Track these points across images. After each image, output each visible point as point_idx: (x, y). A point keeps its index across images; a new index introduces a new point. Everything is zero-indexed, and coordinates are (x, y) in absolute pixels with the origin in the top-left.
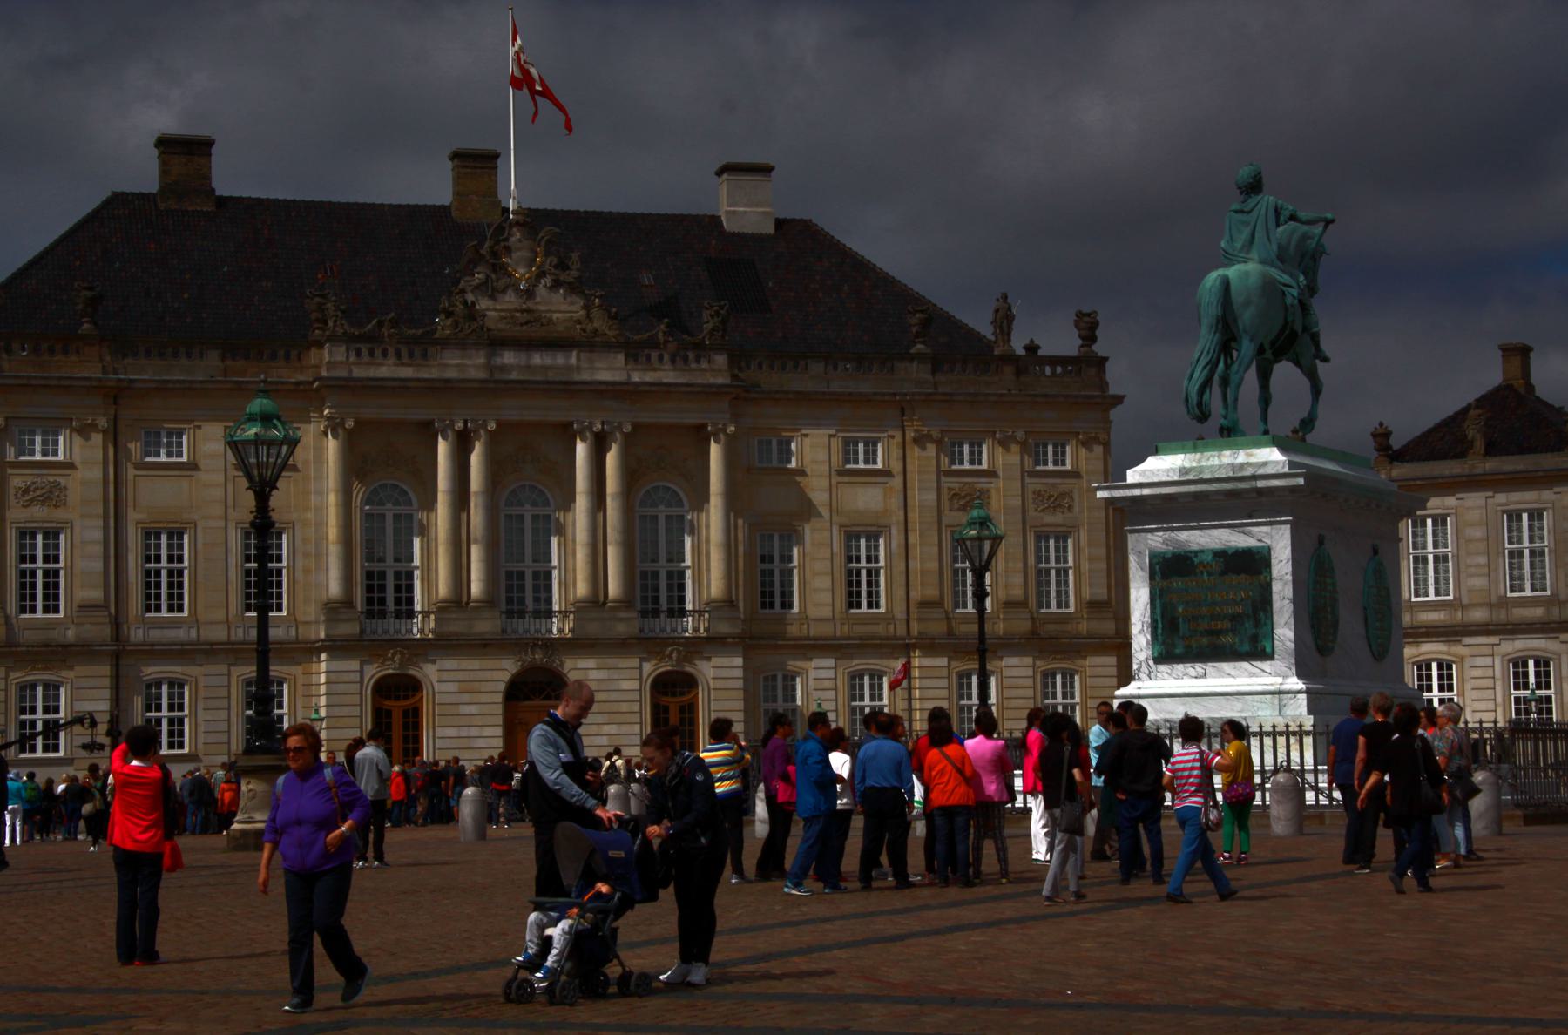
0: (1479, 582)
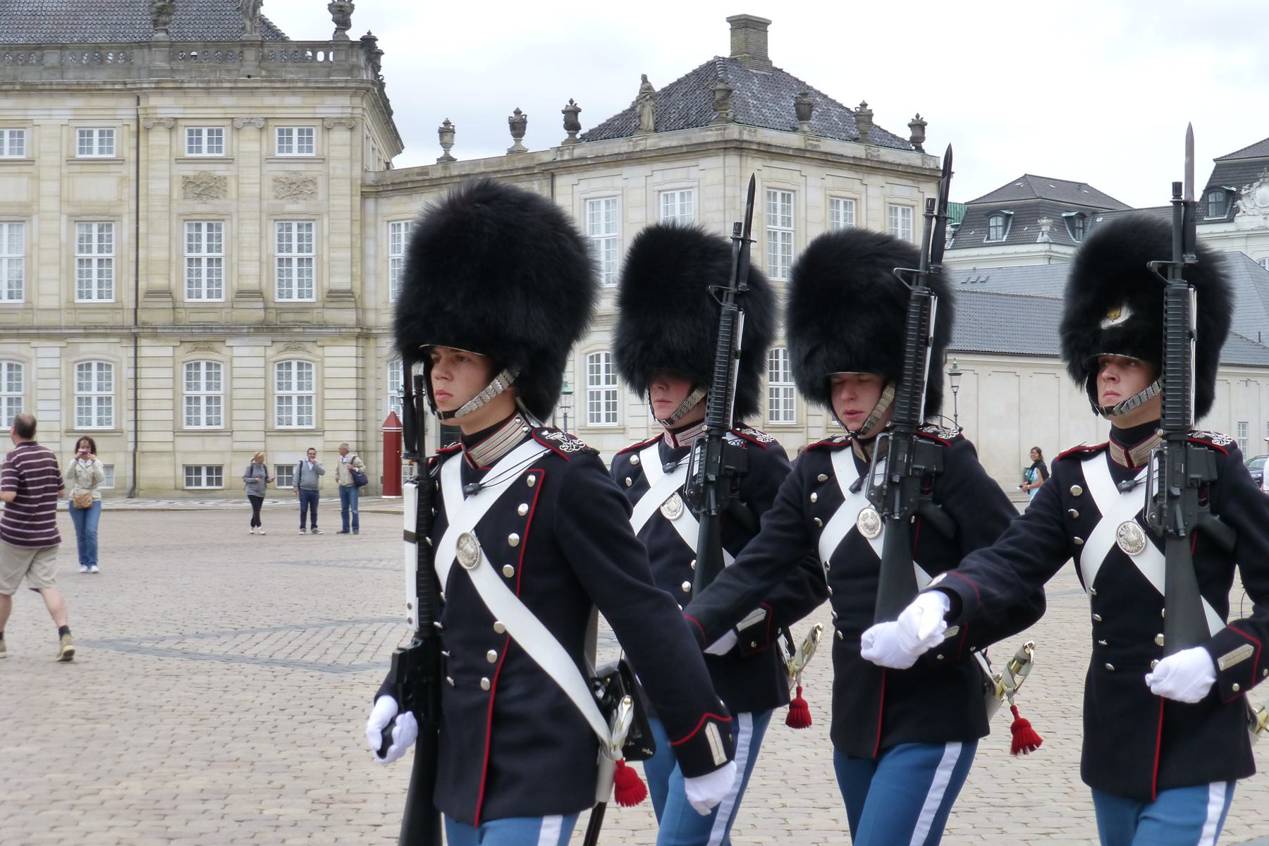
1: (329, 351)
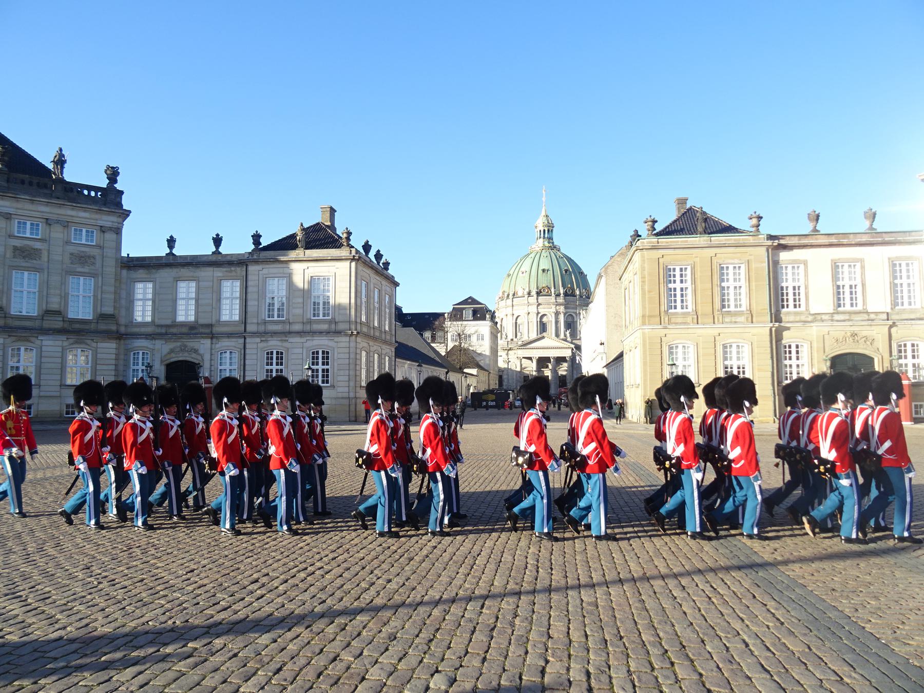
0: (299, 311)
1: (100, 345)
